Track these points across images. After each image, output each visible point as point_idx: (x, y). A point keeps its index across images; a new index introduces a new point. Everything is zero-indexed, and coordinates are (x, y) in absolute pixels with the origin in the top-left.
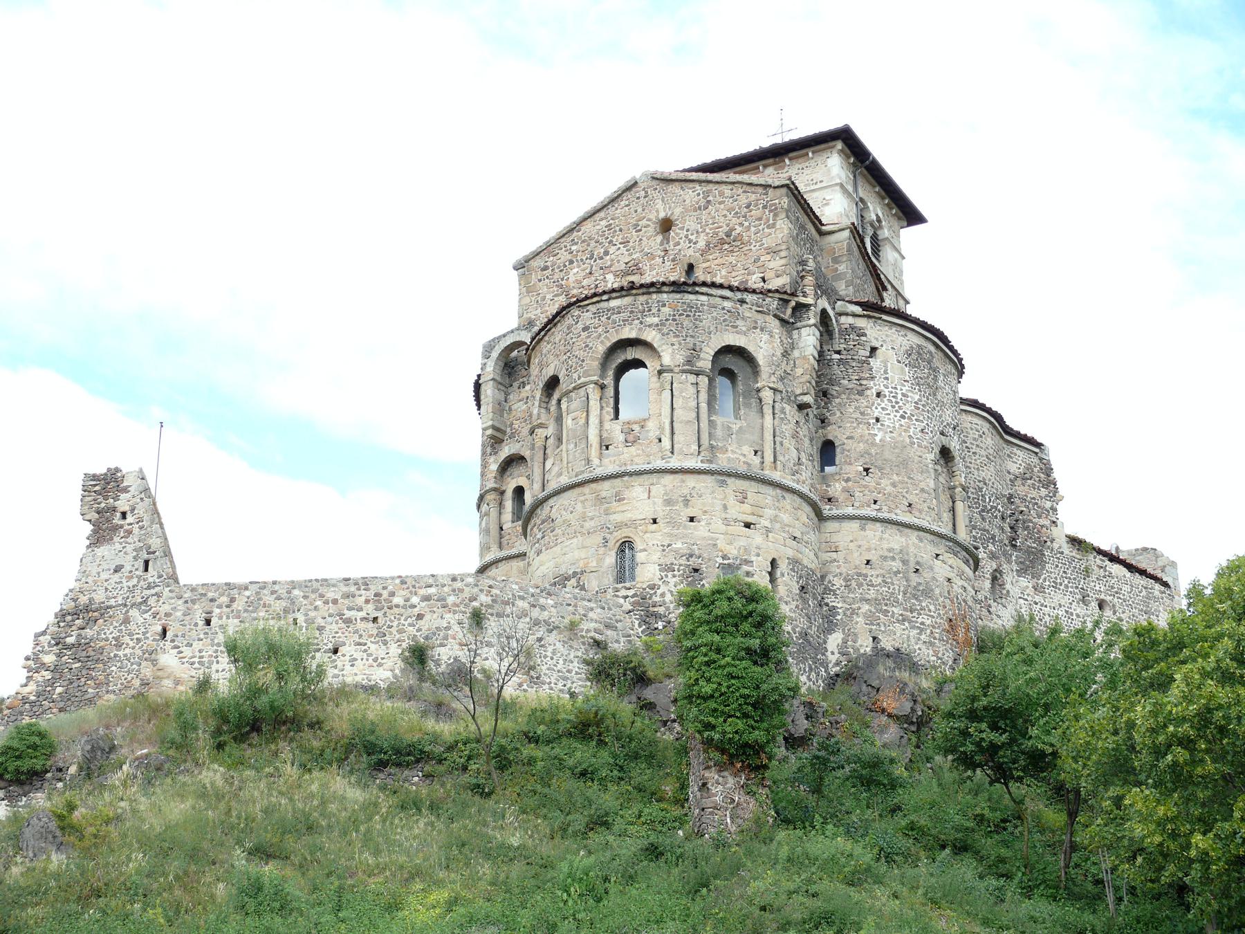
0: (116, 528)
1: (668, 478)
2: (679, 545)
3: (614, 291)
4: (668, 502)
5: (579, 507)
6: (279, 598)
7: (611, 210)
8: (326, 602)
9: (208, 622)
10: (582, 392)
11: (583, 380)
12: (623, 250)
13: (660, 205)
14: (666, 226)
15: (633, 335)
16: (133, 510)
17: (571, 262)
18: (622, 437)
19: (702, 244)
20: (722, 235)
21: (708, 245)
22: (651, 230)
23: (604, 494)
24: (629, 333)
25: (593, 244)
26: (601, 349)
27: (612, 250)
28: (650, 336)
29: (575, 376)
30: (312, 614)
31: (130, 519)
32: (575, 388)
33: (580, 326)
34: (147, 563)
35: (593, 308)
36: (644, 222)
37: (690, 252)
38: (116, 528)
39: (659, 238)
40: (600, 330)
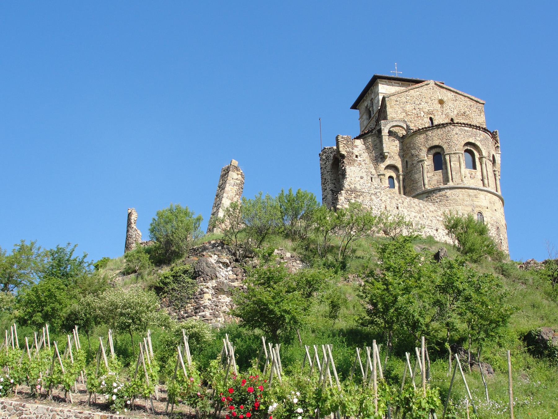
0: (355, 161)
1: (489, 194)
2: (494, 218)
3: (467, 124)
4: (490, 203)
5: (461, 195)
6: (416, 205)
7: (420, 89)
8: (430, 211)
9: (397, 208)
10: (457, 155)
11: (457, 151)
12: (426, 105)
13: (439, 94)
14: (441, 102)
15: (473, 142)
16: (360, 156)
17: (407, 102)
18: (469, 175)
19: (456, 113)
20: (462, 112)
21: (458, 114)
22: (437, 102)
23: (471, 194)
24: (472, 140)
25: (415, 99)
26: (463, 143)
27: (423, 103)
28: (478, 144)
29: (454, 149)
30: (428, 215)
31: (359, 159)
32: (454, 153)
33: (454, 132)
34: (371, 178)
35: (459, 128)
36: (433, 98)
37: (452, 114)
38: (355, 161)
39: (440, 105)
40: (462, 136)
